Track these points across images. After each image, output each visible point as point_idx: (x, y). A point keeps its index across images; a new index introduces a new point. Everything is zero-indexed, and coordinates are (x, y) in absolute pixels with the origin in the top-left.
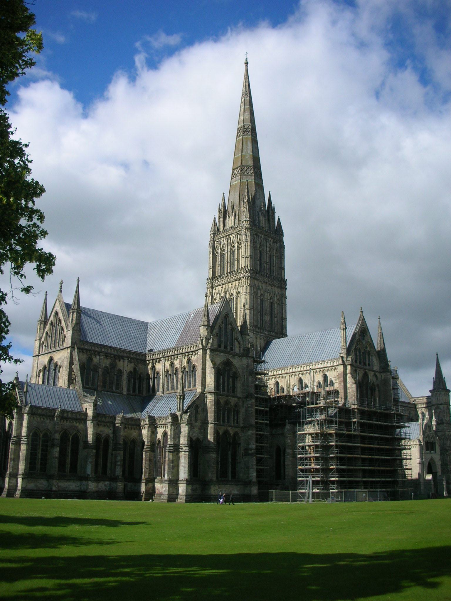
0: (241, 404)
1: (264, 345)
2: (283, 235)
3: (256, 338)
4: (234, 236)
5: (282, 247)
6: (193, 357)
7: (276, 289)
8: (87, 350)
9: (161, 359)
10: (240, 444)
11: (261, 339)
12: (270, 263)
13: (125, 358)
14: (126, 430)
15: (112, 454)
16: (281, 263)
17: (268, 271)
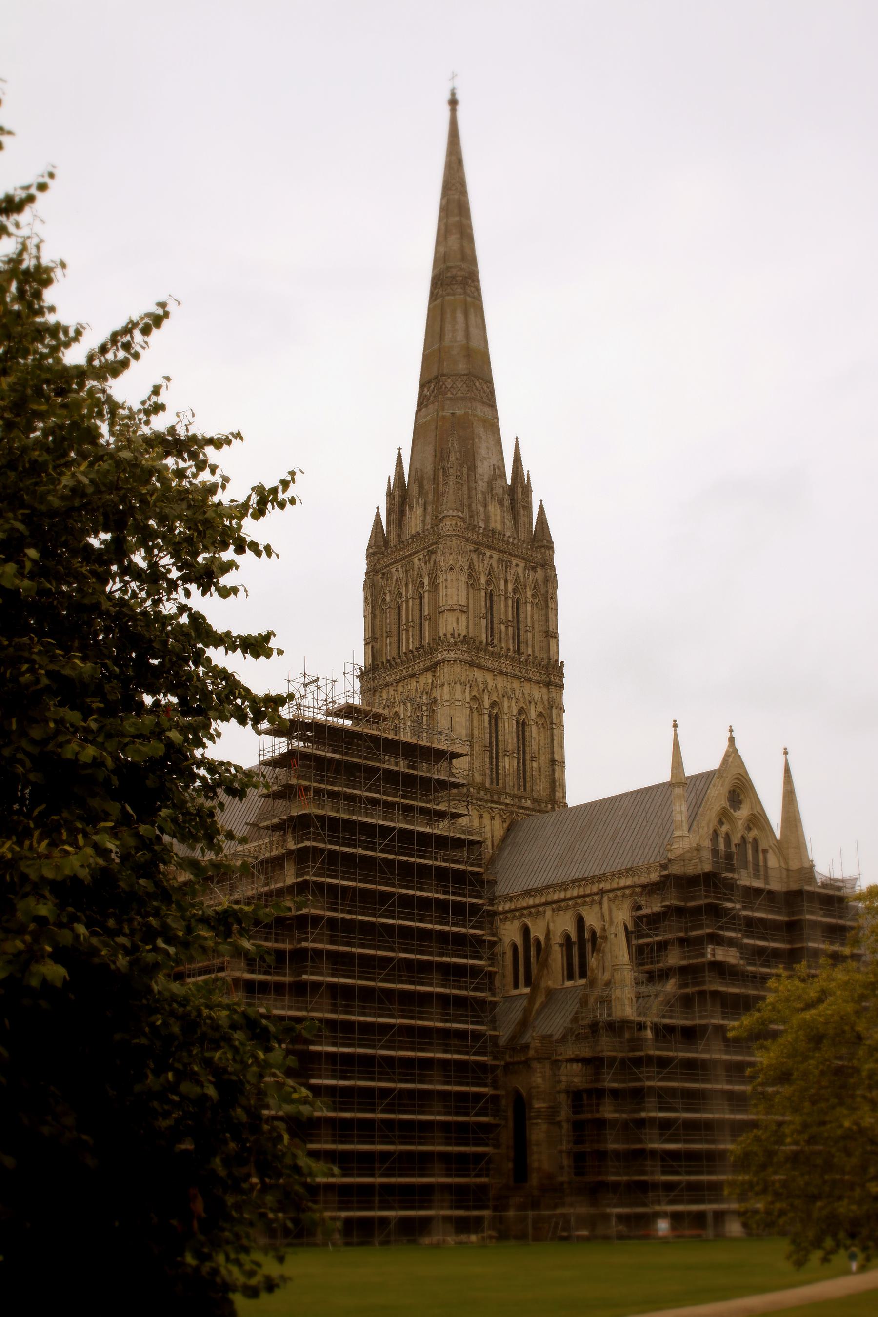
1: (502, 833)
2: (553, 548)
4: (421, 557)
5: (550, 580)
7: (535, 688)
11: (493, 818)
12: (518, 622)
16: (547, 620)
17: (511, 642)
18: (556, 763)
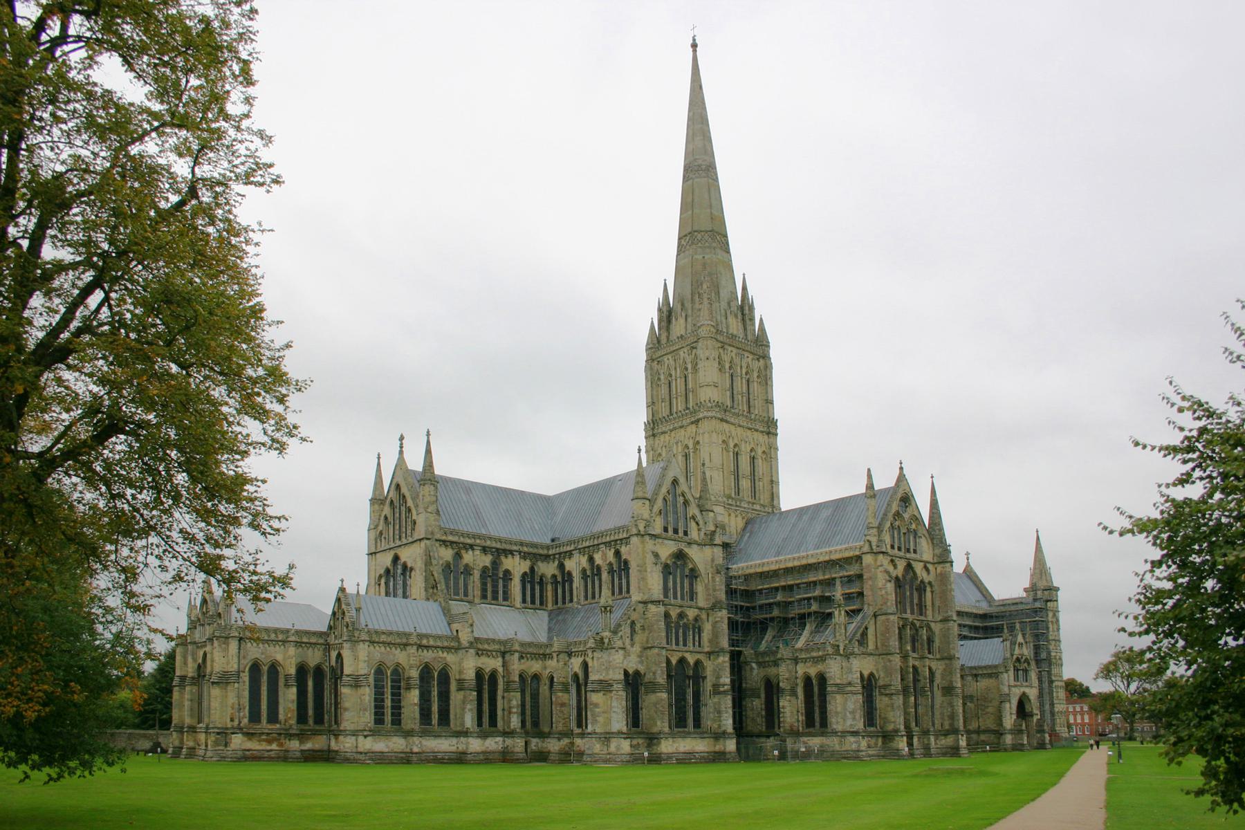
0: (704, 616)
3: (730, 515)
4: (686, 351)
5: (768, 367)
6: (623, 547)
7: (760, 435)
8: (452, 543)
9: (573, 552)
10: (706, 677)
11: (736, 516)
13: (515, 553)
14: (522, 661)
15: (503, 697)
16: (767, 393)
17: (745, 406)
18: (773, 483)
